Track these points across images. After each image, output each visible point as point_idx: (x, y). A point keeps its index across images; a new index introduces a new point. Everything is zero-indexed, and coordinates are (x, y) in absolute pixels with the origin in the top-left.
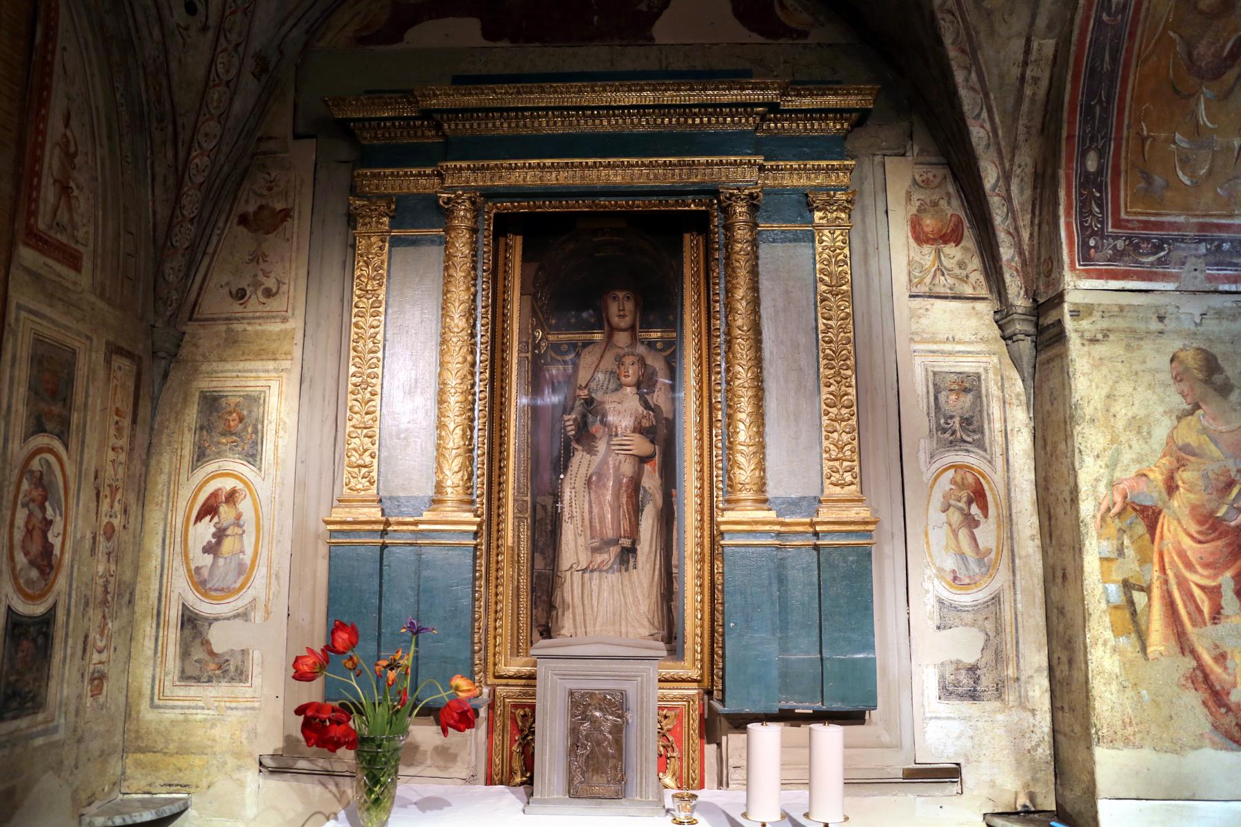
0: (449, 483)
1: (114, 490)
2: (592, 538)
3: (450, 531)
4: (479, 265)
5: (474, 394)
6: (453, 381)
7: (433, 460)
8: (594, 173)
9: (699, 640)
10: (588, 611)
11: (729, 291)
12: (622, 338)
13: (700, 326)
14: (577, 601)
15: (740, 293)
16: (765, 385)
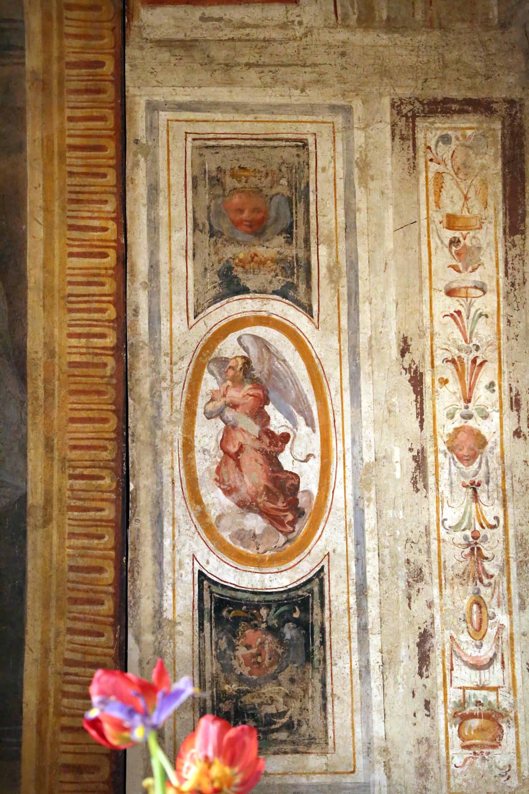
1: (467, 368)
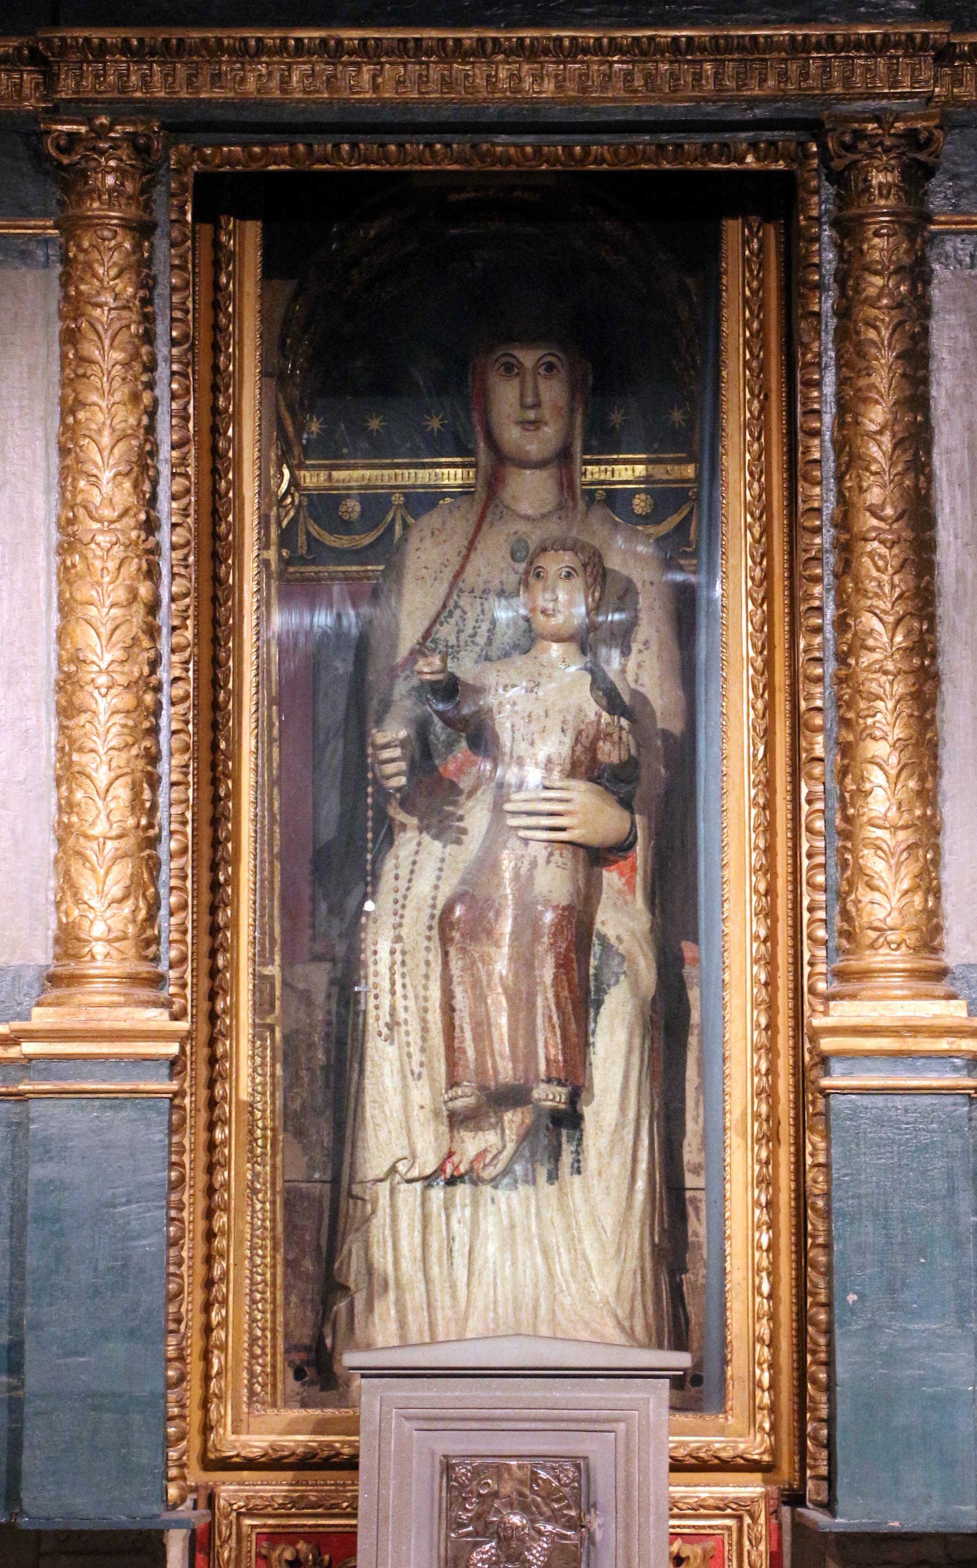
0: (99, 929)
2: (453, 1083)
3: (106, 1057)
4: (161, 328)
5: (158, 689)
6: (102, 654)
7: (49, 870)
8: (478, 72)
9: (764, 1353)
10: (442, 1299)
11: (848, 408)
12: (531, 491)
13: (766, 489)
14: (410, 1268)
15: (876, 416)
16: (943, 664)
